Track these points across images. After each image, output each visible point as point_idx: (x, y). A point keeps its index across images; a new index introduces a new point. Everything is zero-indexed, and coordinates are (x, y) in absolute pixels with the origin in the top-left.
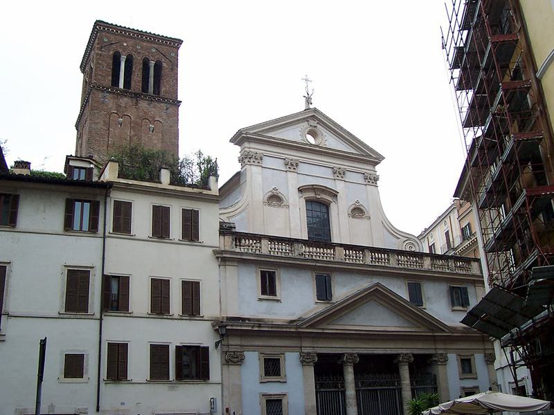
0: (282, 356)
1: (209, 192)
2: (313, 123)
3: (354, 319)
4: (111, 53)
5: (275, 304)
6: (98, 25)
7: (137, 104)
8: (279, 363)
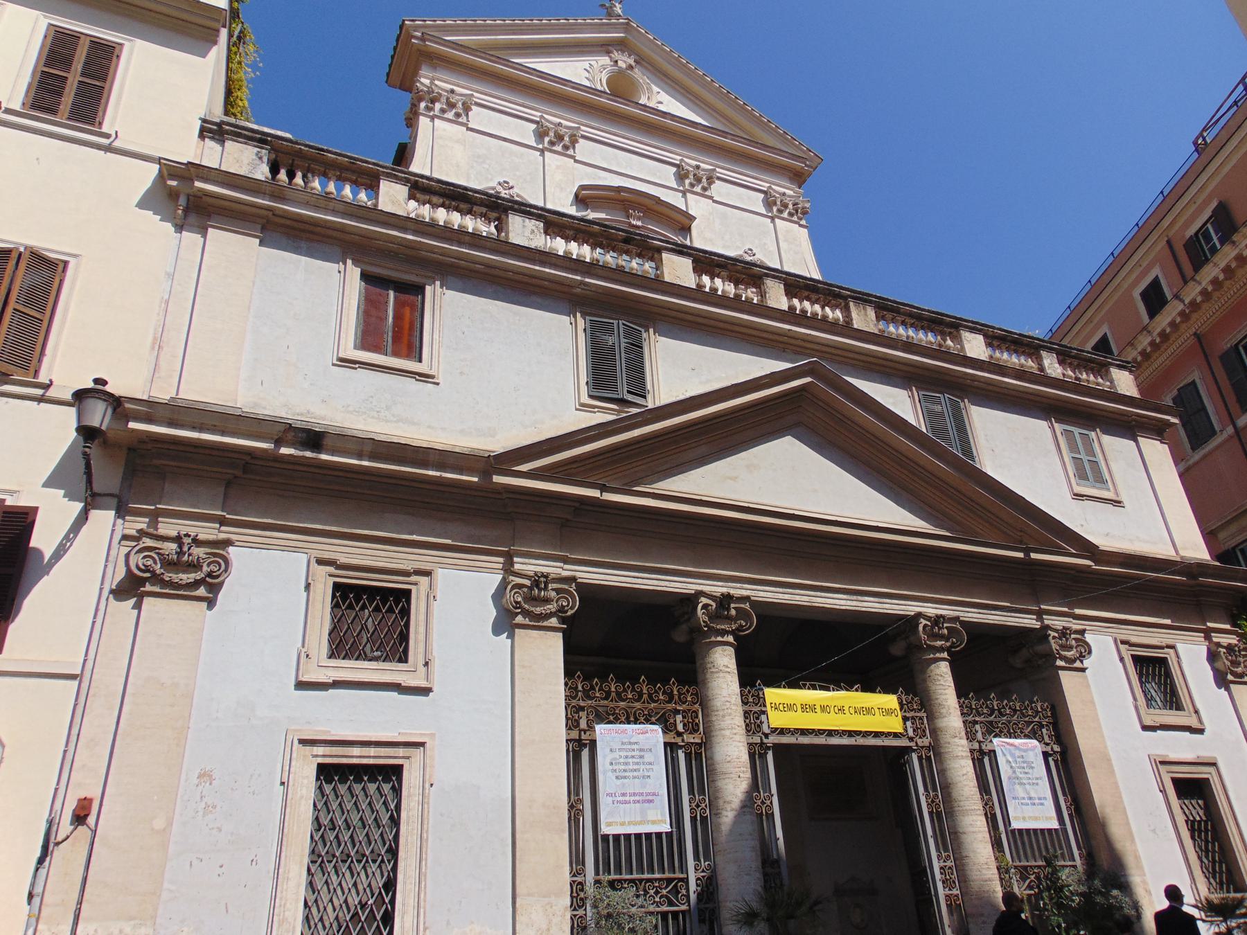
0: (424, 581)
2: (624, 61)
3: (734, 479)
5: (410, 383)
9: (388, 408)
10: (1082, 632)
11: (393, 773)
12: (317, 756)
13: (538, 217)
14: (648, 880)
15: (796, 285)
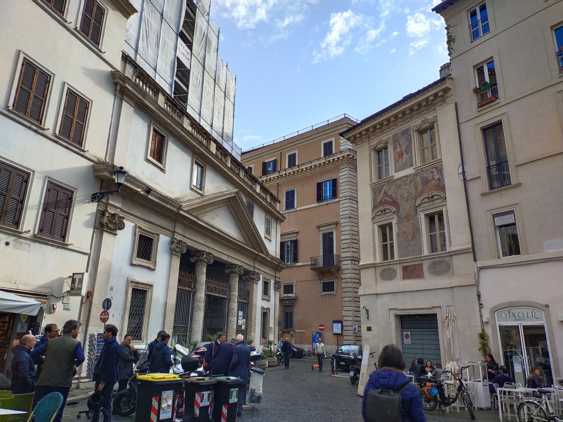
3: (214, 218)
8: (151, 246)
9: (155, 179)
10: (260, 274)
11: (145, 292)
12: (132, 286)
13: (190, 119)
14: (181, 327)
15: (234, 160)
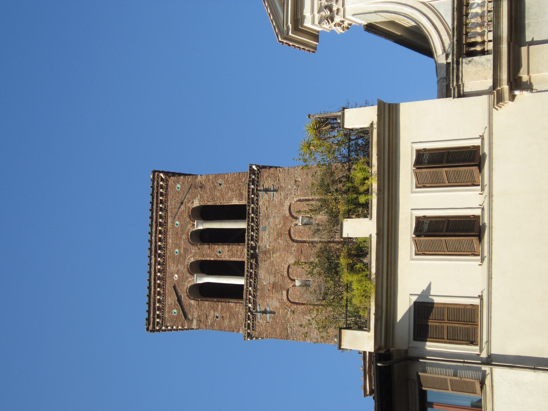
1: (375, 126)
4: (192, 302)
6: (154, 327)
7: (265, 253)
